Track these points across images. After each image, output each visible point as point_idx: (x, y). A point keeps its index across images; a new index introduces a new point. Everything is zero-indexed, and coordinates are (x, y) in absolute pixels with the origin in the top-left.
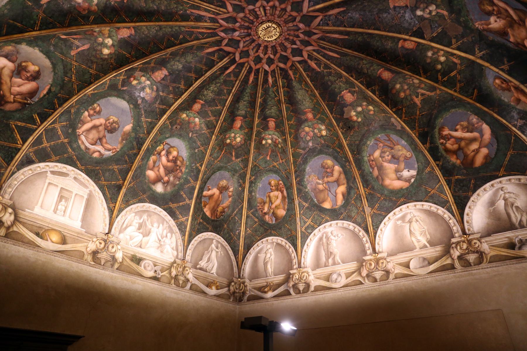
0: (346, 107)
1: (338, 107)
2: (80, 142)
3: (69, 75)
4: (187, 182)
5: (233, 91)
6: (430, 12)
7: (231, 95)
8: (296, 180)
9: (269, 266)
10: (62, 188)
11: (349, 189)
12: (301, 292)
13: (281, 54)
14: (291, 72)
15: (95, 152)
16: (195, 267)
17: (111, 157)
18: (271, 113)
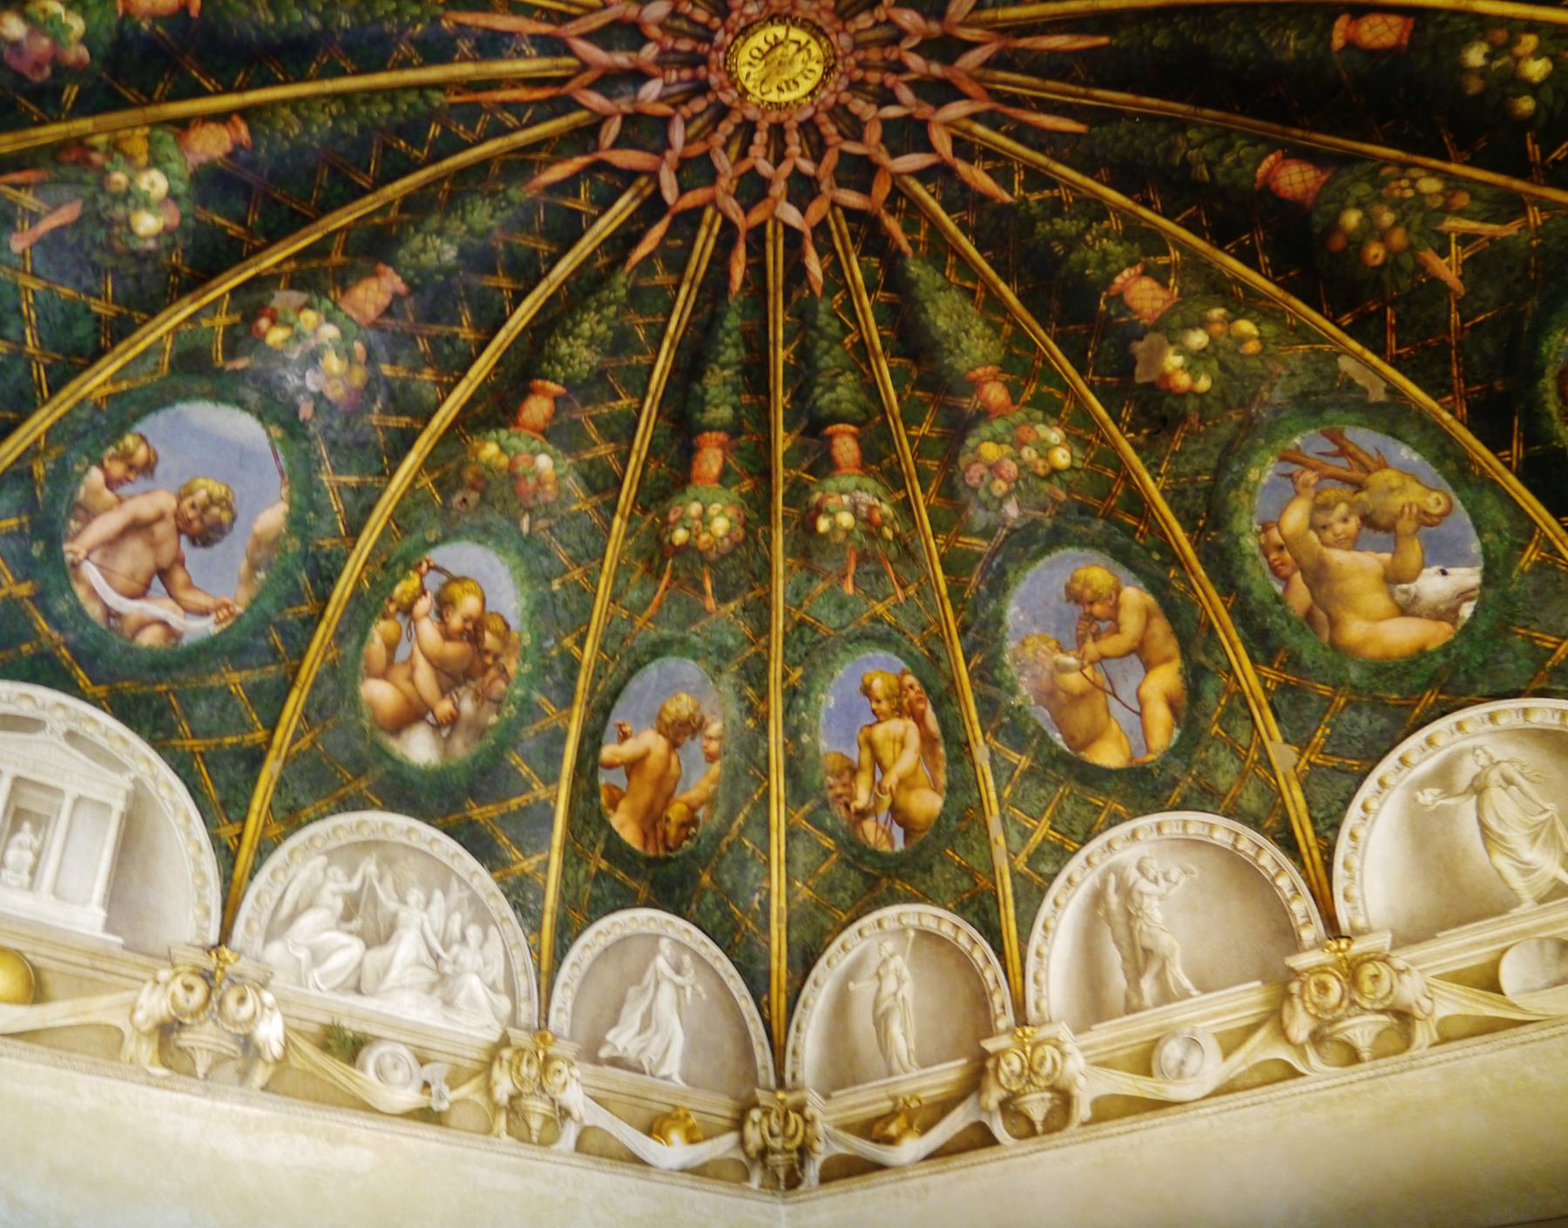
0: (1140, 339)
1: (1105, 344)
2: (81, 592)
3: (11, 332)
4: (530, 711)
5: (672, 328)
7: (666, 344)
8: (967, 663)
9: (896, 1030)
10: (18, 781)
11: (1194, 676)
12: (1039, 1128)
13: (842, 153)
14: (892, 224)
15: (143, 625)
16: (591, 1054)
17: (213, 640)
18: (838, 402)
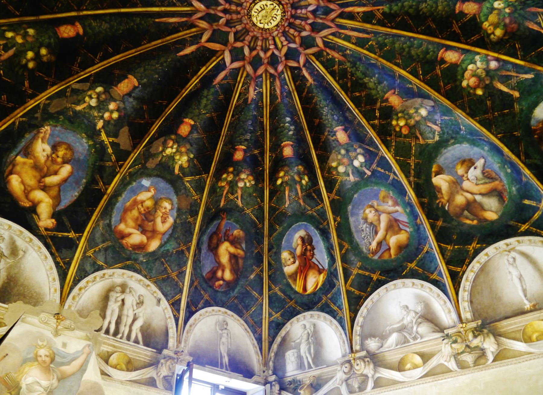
6: (91, 97)
